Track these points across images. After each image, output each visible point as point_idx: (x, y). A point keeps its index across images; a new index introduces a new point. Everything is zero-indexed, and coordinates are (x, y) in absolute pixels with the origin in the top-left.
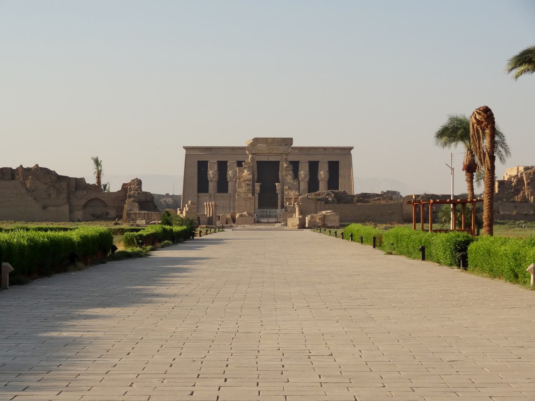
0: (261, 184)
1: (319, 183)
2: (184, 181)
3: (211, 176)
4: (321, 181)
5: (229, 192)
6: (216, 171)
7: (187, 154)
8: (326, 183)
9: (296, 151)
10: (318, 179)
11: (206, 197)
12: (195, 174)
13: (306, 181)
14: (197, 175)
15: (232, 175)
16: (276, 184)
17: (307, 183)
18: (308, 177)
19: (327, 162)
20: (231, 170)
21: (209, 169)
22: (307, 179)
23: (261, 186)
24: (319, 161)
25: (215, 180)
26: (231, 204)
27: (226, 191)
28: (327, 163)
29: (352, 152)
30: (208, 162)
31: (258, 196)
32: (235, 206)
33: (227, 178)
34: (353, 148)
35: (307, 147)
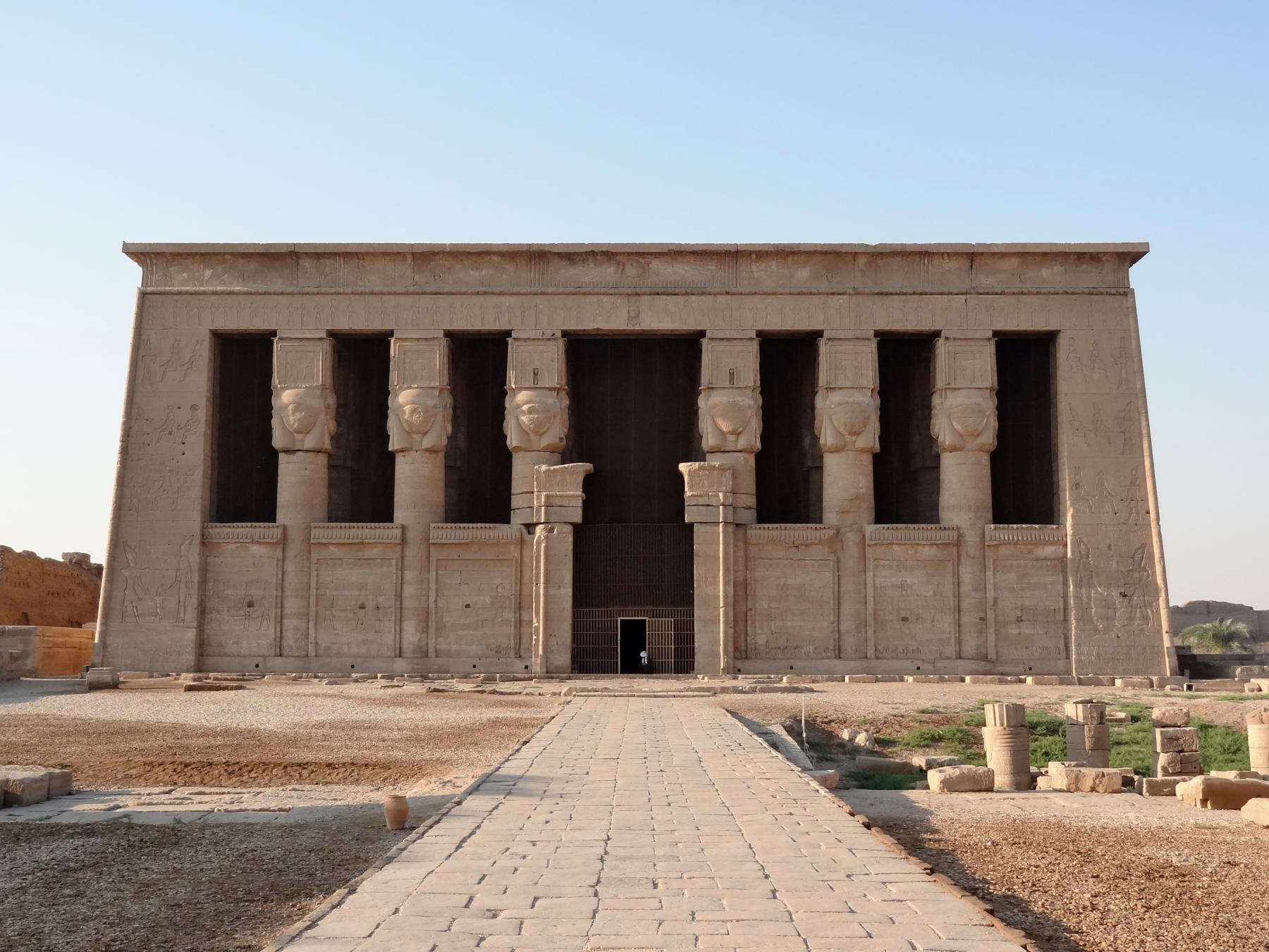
0: (588, 466)
1: (938, 457)
2: (125, 451)
3: (293, 419)
4: (953, 449)
5: (400, 515)
6: (323, 387)
7: (149, 289)
8: (985, 459)
9: (803, 273)
10: (931, 441)
11: (255, 549)
12: (194, 408)
13: (863, 451)
14: (203, 414)
15: (415, 416)
16: (683, 467)
17: (867, 460)
18: (874, 427)
19: (991, 336)
20: (409, 388)
21: (275, 381)
22: (870, 438)
23: (589, 483)
24: (937, 334)
25: (310, 442)
26: (409, 590)
27: (383, 512)
28: (989, 339)
29: (1137, 274)
30: (275, 340)
31: (570, 539)
32: (432, 605)
33: (388, 437)
34: (1144, 253)
35: (867, 245)
